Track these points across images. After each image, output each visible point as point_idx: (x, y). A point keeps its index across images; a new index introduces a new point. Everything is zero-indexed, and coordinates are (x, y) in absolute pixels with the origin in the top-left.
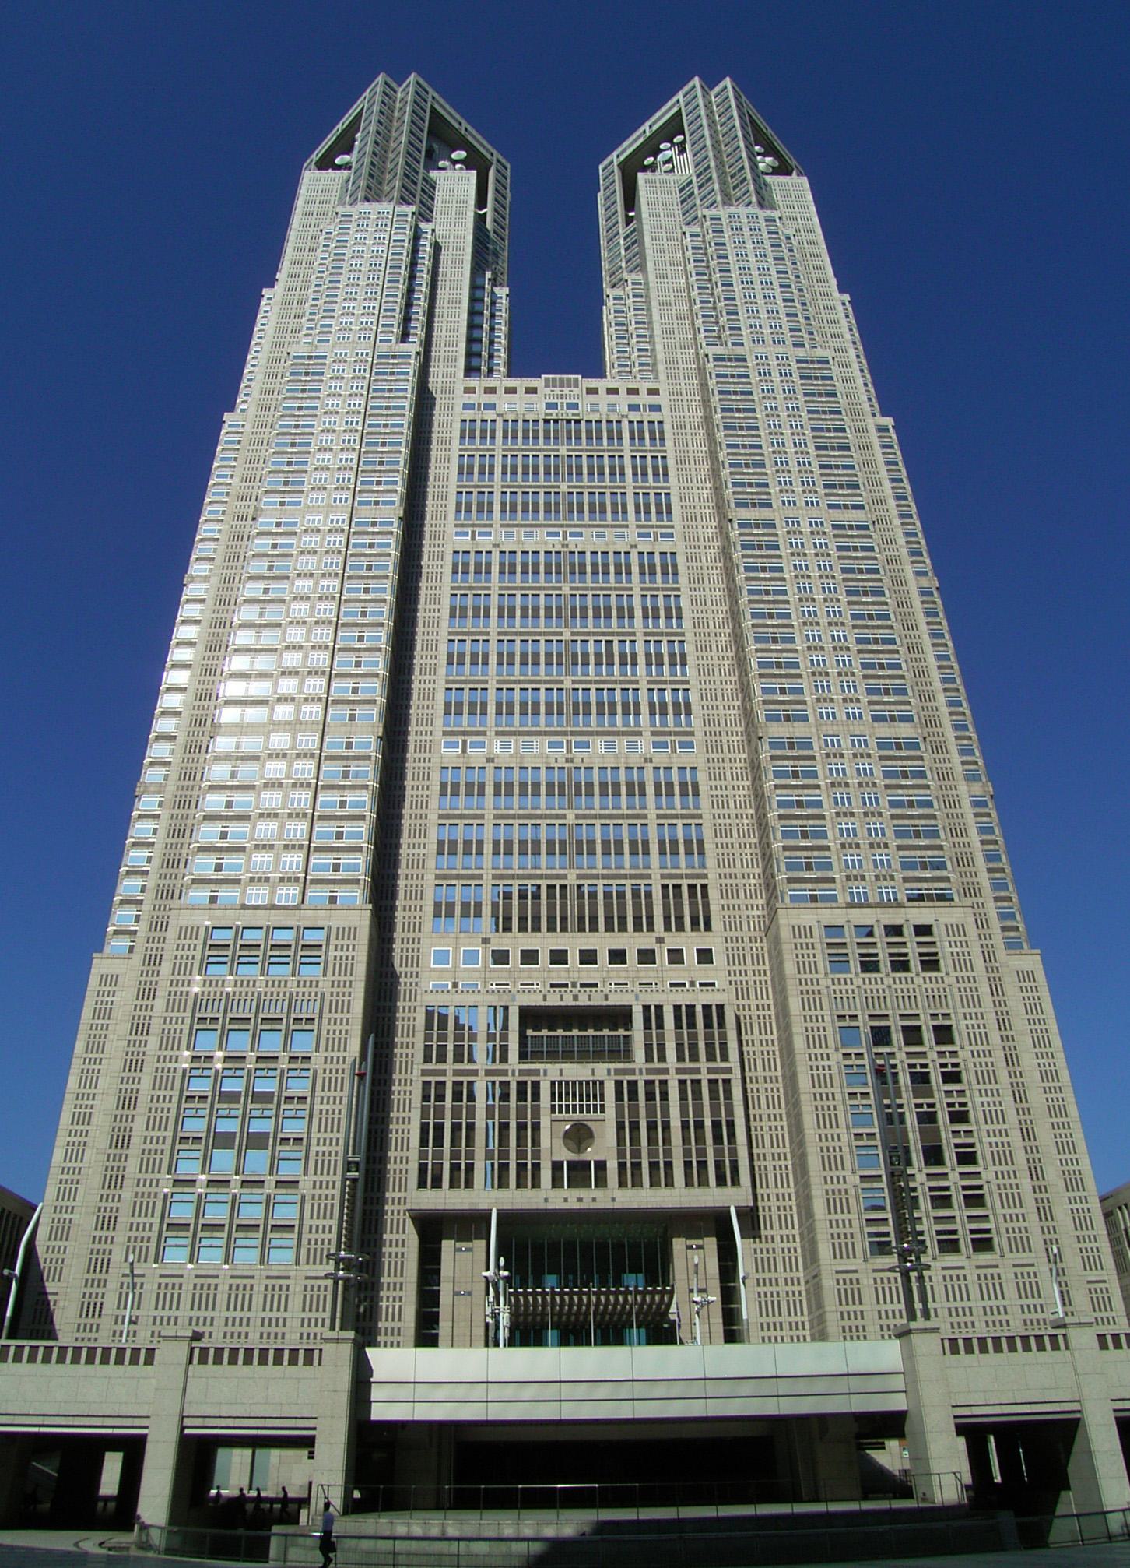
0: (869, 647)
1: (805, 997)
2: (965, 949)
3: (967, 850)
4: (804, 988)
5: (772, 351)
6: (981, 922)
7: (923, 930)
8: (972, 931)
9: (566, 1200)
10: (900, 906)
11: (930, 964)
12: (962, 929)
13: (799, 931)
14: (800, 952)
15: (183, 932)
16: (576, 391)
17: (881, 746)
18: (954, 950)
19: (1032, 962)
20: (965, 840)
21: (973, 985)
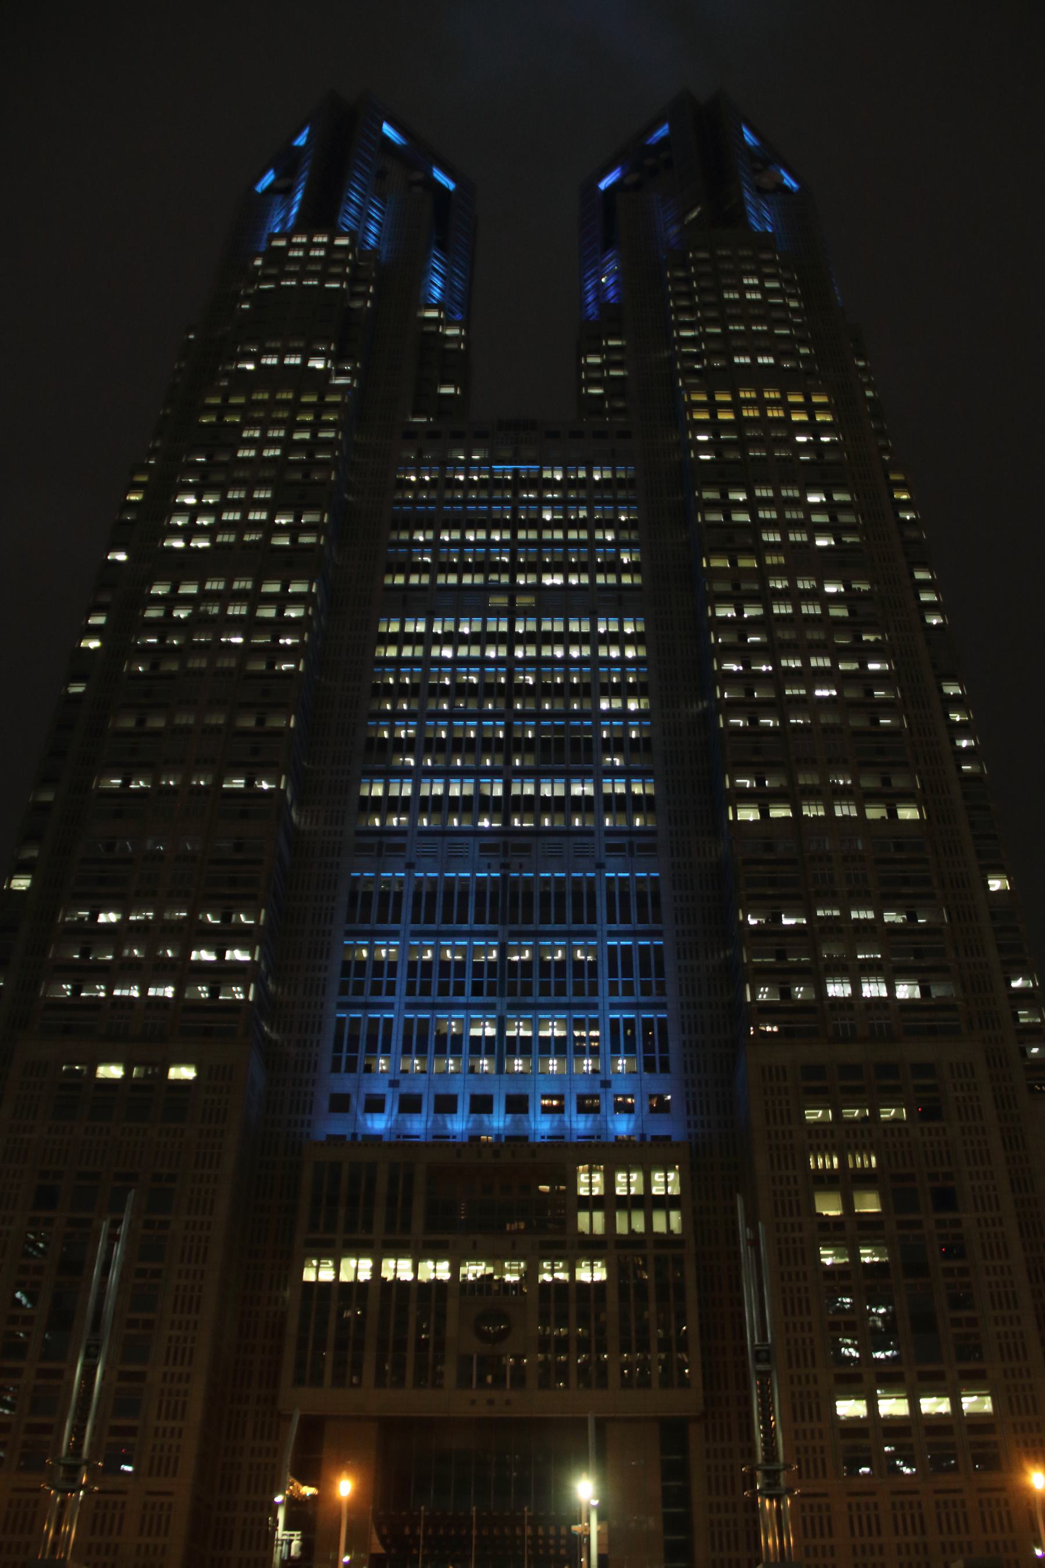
9: (473, 1402)
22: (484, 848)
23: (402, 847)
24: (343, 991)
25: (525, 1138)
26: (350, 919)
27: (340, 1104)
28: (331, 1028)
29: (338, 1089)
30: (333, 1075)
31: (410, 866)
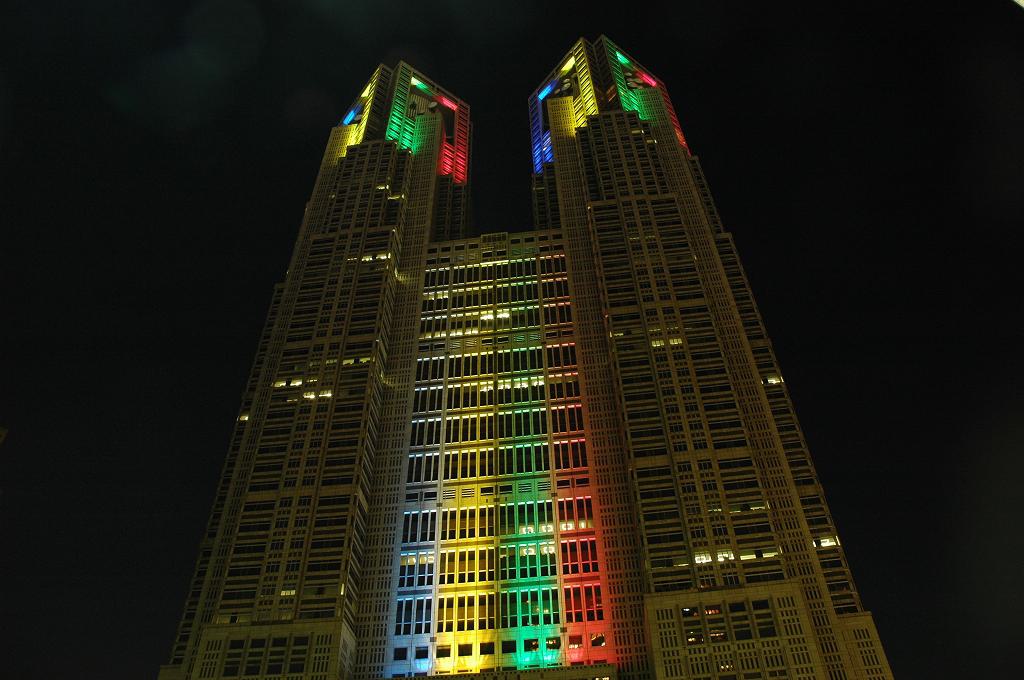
0: (711, 394)
1: (668, 666)
2: (794, 617)
3: (800, 538)
4: (667, 658)
5: (633, 198)
6: (811, 594)
7: (761, 604)
8: (800, 603)
10: (741, 586)
11: (769, 631)
12: (791, 601)
13: (662, 614)
14: (663, 630)
15: (211, 645)
16: (504, 243)
17: (722, 466)
18: (786, 618)
19: (865, 621)
20: (798, 530)
21: (802, 645)
22: (483, 490)
23: (434, 495)
24: (401, 584)
25: (515, 668)
26: (405, 540)
27: (401, 654)
28: (394, 608)
29: (399, 646)
30: (396, 637)
31: (439, 505)
